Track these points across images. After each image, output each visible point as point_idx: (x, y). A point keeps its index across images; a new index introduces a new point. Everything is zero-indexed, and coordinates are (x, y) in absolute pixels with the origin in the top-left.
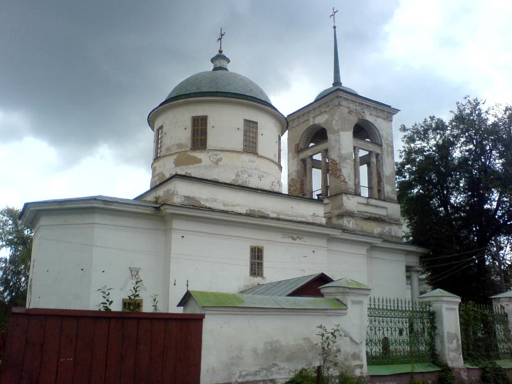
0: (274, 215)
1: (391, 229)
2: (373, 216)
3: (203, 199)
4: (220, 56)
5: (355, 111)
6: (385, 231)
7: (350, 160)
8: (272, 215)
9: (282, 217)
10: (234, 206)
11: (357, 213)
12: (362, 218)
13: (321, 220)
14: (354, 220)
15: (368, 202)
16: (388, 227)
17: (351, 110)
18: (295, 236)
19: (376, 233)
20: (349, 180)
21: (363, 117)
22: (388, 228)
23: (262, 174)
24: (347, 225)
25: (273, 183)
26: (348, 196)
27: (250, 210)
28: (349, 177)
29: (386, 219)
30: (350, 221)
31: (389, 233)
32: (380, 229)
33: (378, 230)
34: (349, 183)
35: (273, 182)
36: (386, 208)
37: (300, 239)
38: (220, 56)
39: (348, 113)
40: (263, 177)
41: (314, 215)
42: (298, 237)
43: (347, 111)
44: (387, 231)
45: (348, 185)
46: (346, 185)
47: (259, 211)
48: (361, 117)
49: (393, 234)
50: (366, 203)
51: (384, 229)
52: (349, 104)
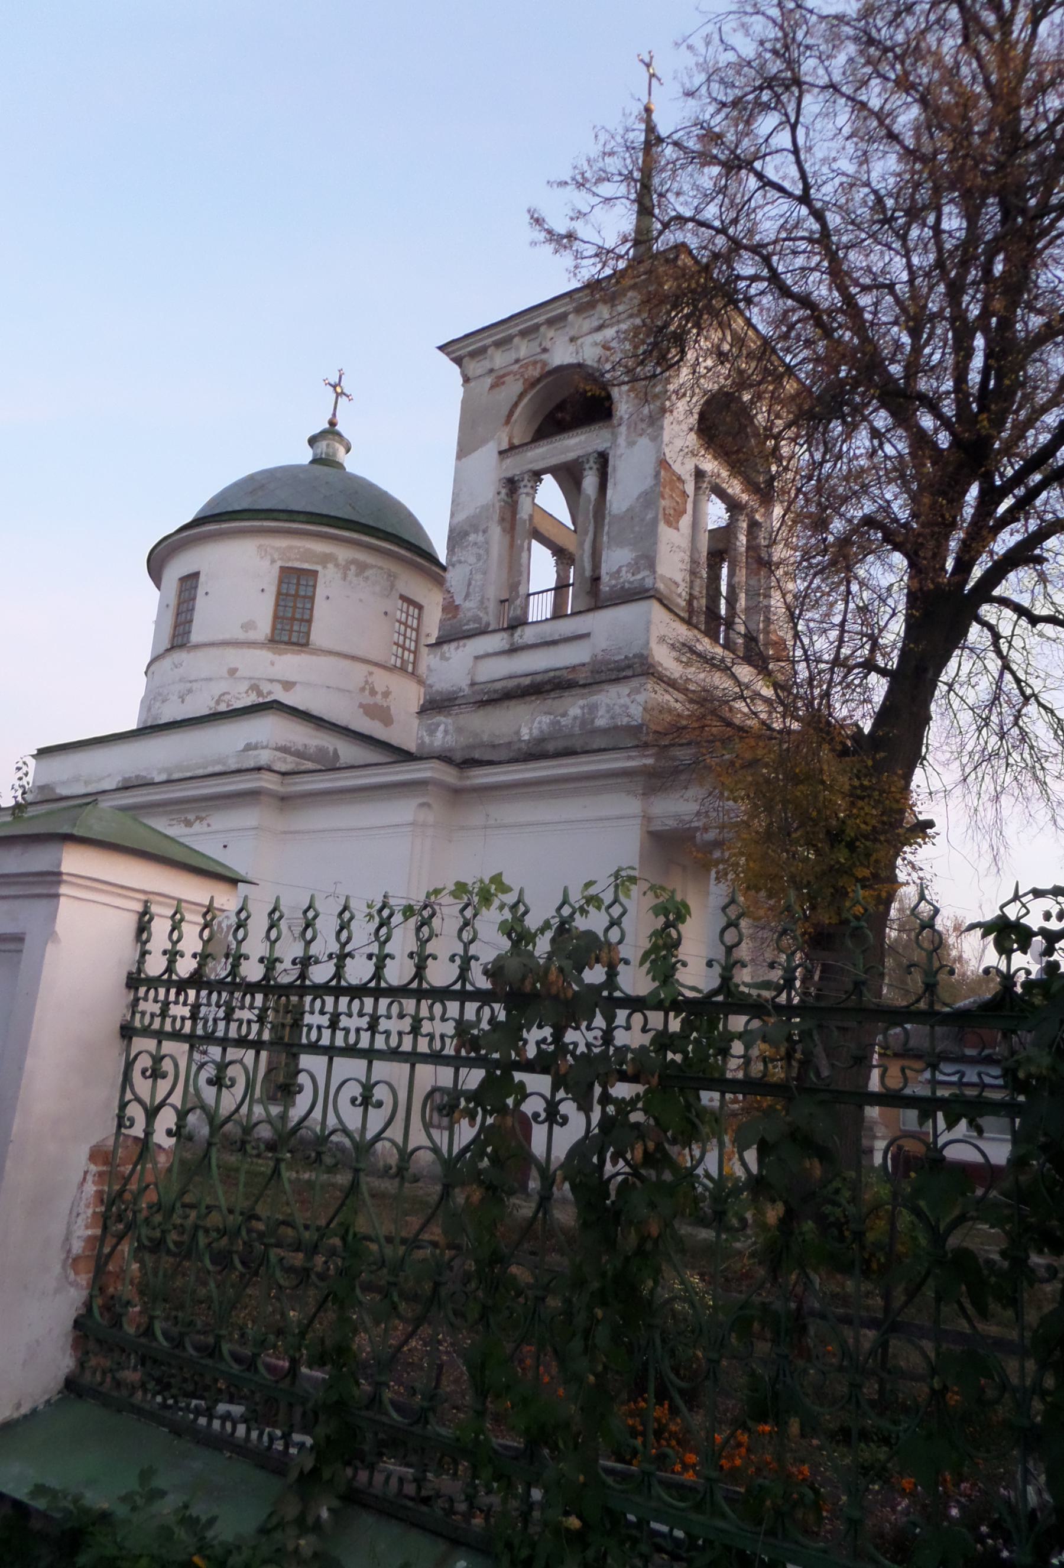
0: (163, 777)
1: (593, 708)
2: (527, 681)
3: (63, 783)
4: (331, 432)
5: (517, 366)
6: (564, 721)
7: (476, 531)
8: (157, 780)
9: (176, 776)
10: (100, 780)
11: (467, 691)
12: (482, 701)
13: (256, 756)
14: (450, 721)
15: (512, 644)
16: (581, 702)
17: (501, 373)
18: (191, 817)
19: (526, 737)
20: (467, 596)
21: (545, 364)
22: (582, 708)
23: (189, 685)
24: (427, 739)
25: (226, 697)
26: (445, 647)
27: (125, 779)
28: (469, 584)
29: (582, 677)
30: (438, 725)
31: (583, 723)
32: (546, 719)
33: (536, 724)
34: (468, 604)
35: (223, 694)
36: (586, 636)
37: (200, 819)
38: (331, 432)
39: (492, 387)
40: (190, 691)
41: (249, 747)
42: (197, 818)
43: (489, 381)
44: (575, 718)
45: (461, 615)
46: (454, 617)
47: (137, 777)
48: (536, 373)
49: (601, 722)
50: (507, 647)
51: (564, 715)
52: (518, 349)
